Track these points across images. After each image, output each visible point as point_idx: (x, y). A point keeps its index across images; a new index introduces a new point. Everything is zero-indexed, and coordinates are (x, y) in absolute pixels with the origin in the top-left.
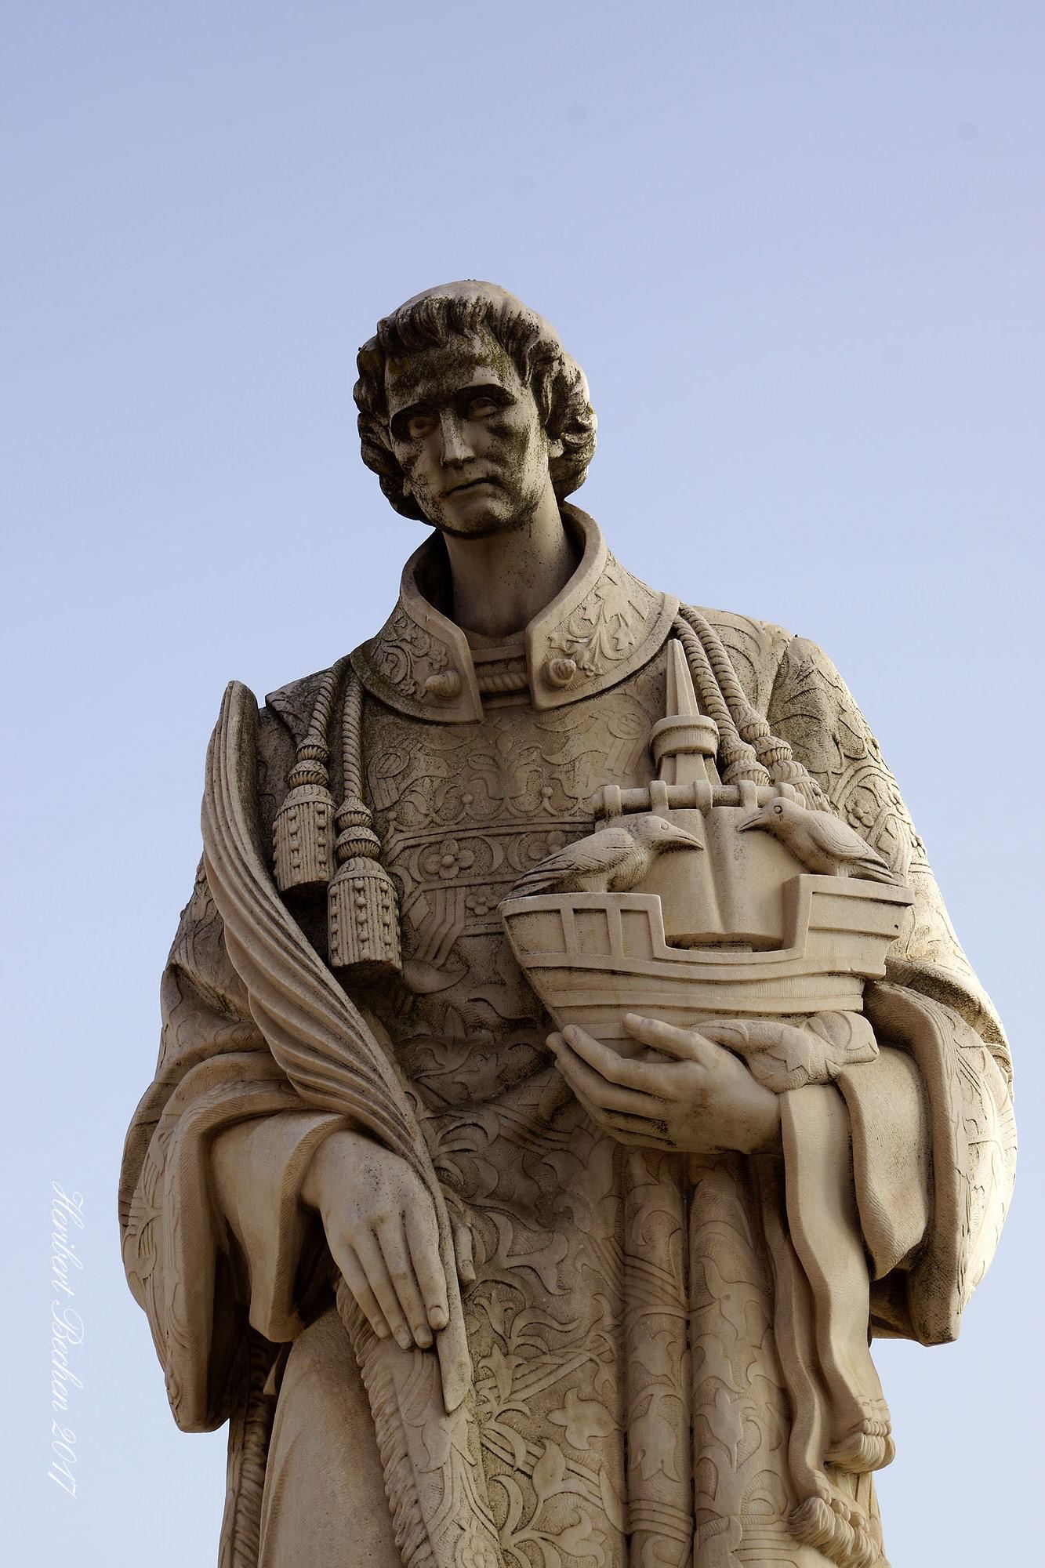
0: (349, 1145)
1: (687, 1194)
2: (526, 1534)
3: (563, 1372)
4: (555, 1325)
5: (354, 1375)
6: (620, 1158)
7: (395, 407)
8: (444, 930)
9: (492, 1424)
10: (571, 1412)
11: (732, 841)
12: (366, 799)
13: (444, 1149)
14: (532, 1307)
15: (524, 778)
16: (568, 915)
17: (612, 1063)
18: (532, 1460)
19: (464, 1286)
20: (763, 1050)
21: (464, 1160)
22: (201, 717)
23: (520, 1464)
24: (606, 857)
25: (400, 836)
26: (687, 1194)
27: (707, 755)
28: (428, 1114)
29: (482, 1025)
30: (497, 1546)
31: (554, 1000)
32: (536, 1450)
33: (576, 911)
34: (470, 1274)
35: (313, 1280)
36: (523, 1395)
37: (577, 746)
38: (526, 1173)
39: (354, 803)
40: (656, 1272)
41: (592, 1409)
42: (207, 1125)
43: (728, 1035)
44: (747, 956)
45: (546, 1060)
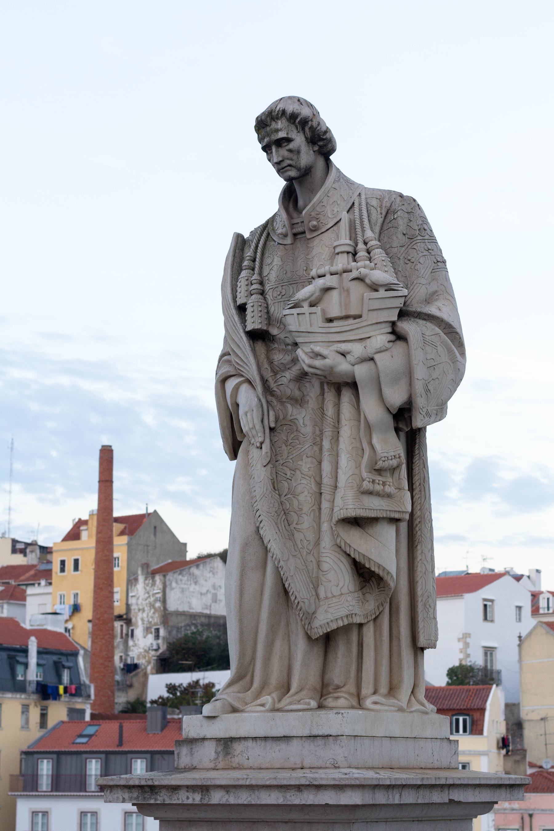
0: (245, 388)
2: (289, 496)
3: (303, 449)
4: (302, 436)
6: (322, 385)
8: (278, 316)
9: (281, 467)
10: (304, 461)
12: (260, 274)
13: (275, 385)
14: (297, 431)
15: (301, 264)
16: (296, 315)
17: (307, 360)
18: (292, 476)
19: (271, 429)
20: (348, 353)
21: (281, 387)
22: (224, 247)
23: (288, 477)
24: (308, 295)
25: (268, 285)
27: (348, 253)
28: (272, 374)
29: (288, 345)
30: (279, 500)
31: (298, 340)
32: (293, 472)
33: (298, 314)
34: (273, 425)
36: (291, 457)
37: (314, 252)
38: (299, 389)
39: (256, 277)
40: (328, 418)
41: (309, 459)
42: (221, 378)
43: (339, 349)
44: (351, 321)
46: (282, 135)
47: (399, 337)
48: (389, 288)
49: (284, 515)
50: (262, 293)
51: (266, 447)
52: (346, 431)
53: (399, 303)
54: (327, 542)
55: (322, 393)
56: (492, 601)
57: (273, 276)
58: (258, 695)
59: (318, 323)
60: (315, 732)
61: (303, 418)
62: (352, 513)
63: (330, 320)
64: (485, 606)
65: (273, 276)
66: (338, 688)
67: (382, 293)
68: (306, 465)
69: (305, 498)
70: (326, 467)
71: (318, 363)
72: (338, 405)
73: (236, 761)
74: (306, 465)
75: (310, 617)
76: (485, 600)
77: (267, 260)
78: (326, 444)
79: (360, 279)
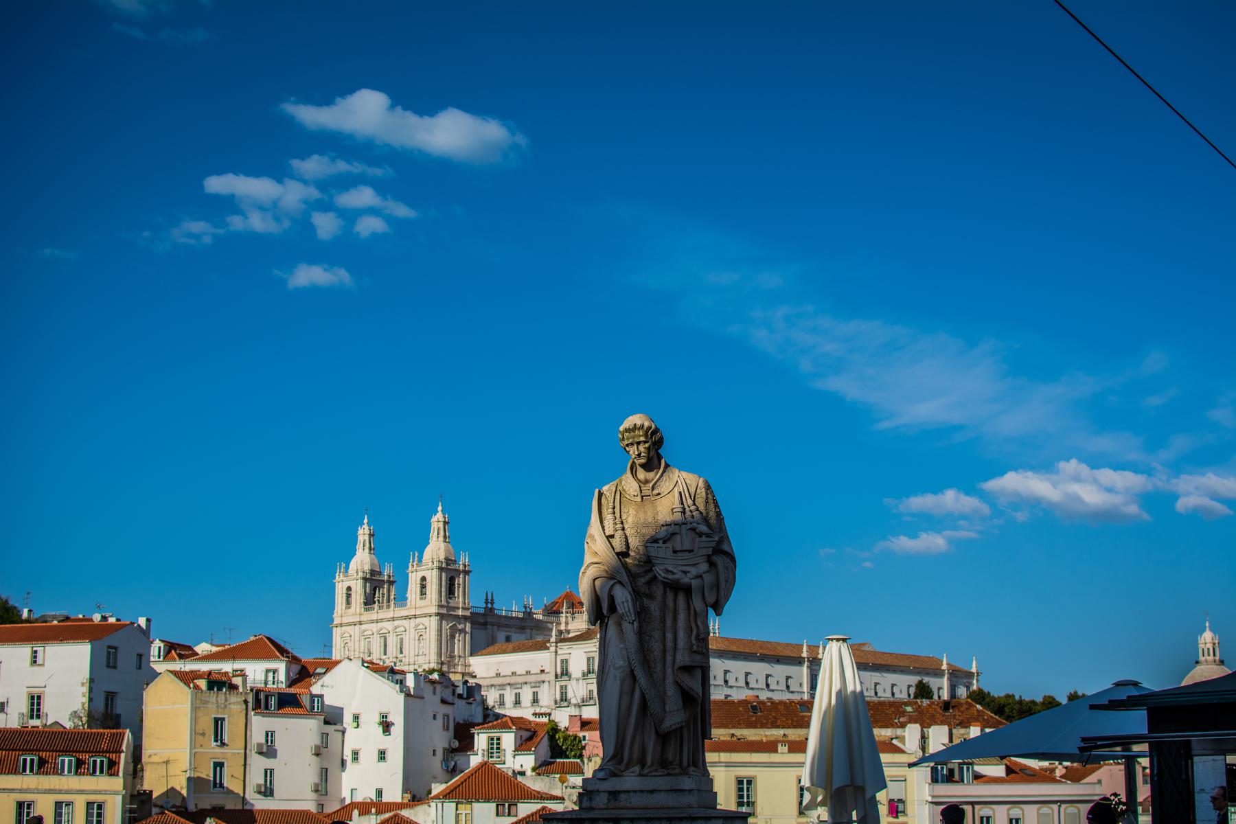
1: (676, 595)
5: (620, 625)
7: (626, 442)
11: (684, 532)
26: (676, 595)
35: (613, 608)
45: (651, 570)
46: (642, 439)
47: (712, 564)
48: (708, 535)
49: (646, 662)
50: (623, 529)
51: (636, 624)
52: (682, 617)
53: (713, 544)
54: (670, 680)
55: (665, 592)
56: (116, 648)
57: (630, 520)
58: (627, 768)
59: (670, 554)
60: (675, 787)
61: (654, 607)
62: (688, 664)
63: (675, 552)
64: (109, 653)
65: (630, 520)
66: (671, 763)
67: (704, 538)
68: (657, 635)
69: (657, 654)
70: (669, 636)
71: (670, 577)
72: (675, 601)
73: (622, 804)
74: (657, 635)
75: (662, 721)
76: (109, 647)
77: (624, 510)
78: (669, 622)
79: (693, 529)
